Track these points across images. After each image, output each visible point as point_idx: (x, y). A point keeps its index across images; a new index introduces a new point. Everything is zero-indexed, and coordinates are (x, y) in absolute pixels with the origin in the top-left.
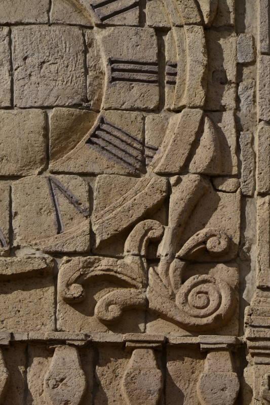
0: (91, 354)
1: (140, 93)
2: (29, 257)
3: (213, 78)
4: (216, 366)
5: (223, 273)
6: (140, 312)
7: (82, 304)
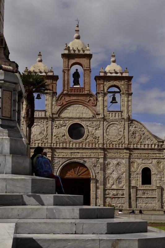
0: (42, 143)
1: (44, 131)
2: (39, 139)
3: (47, 130)
4: (47, 144)
5: (47, 140)
6: (43, 142)
7: (41, 141)
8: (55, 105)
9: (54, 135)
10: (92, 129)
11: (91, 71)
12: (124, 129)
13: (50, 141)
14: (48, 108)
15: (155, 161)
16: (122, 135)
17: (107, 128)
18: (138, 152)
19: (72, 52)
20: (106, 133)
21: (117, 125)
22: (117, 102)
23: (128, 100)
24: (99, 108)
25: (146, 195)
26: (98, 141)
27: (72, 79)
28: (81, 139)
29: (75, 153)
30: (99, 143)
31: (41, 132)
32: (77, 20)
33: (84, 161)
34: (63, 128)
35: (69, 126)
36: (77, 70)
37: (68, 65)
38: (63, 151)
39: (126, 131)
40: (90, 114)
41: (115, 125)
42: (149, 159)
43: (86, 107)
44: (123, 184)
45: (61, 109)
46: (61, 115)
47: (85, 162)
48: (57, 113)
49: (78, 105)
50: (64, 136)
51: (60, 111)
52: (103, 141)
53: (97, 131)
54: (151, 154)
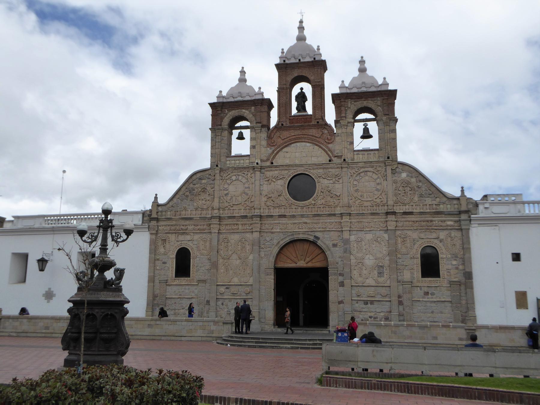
10: (329, 182)
15: (442, 235)
18: (413, 219)
21: (371, 173)
22: (371, 137)
25: (430, 296)
27: (294, 104)
29: (300, 223)
32: (301, 13)
33: (315, 236)
34: (280, 182)
36: (302, 89)
38: (280, 222)
40: (323, 158)
41: (369, 173)
42: (433, 231)
43: (317, 145)
47: (318, 238)
54: (437, 222)
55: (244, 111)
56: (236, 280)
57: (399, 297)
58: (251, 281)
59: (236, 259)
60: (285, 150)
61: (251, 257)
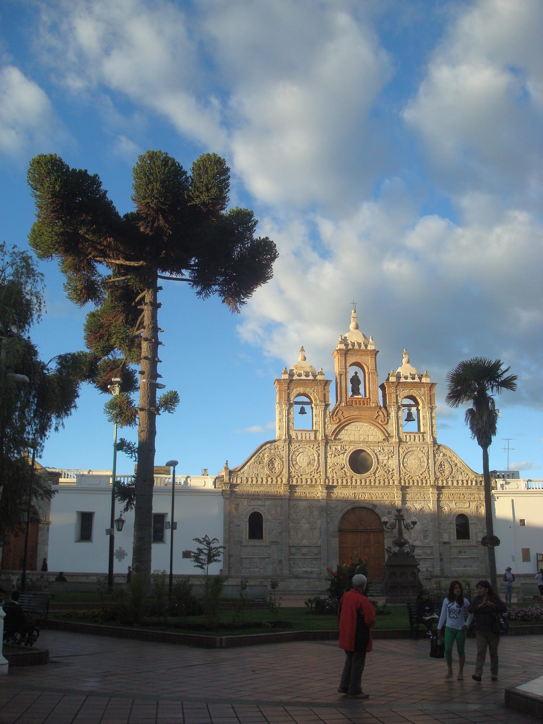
2: (307, 472)
8: (328, 423)
9: (328, 468)
11: (377, 375)
12: (428, 459)
13: (323, 477)
14: (320, 427)
16: (425, 468)
17: (404, 458)
19: (350, 347)
20: (403, 464)
23: (431, 417)
24: (392, 428)
25: (463, 554)
26: (392, 477)
27: (350, 386)
28: (368, 473)
30: (394, 478)
31: (310, 462)
32: (353, 303)
35: (350, 453)
36: (356, 373)
37: (346, 366)
39: (431, 462)
44: (430, 538)
45: (338, 430)
46: (339, 437)
48: (332, 435)
49: (361, 423)
50: (342, 469)
51: (337, 432)
52: (400, 476)
53: (390, 462)
55: (308, 389)
56: (305, 542)
57: (440, 555)
58: (319, 544)
59: (305, 523)
60: (346, 428)
61: (319, 522)
